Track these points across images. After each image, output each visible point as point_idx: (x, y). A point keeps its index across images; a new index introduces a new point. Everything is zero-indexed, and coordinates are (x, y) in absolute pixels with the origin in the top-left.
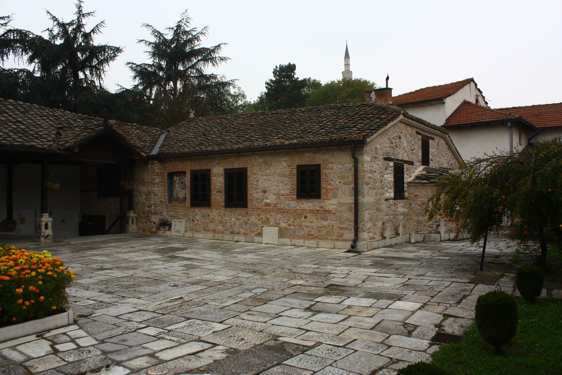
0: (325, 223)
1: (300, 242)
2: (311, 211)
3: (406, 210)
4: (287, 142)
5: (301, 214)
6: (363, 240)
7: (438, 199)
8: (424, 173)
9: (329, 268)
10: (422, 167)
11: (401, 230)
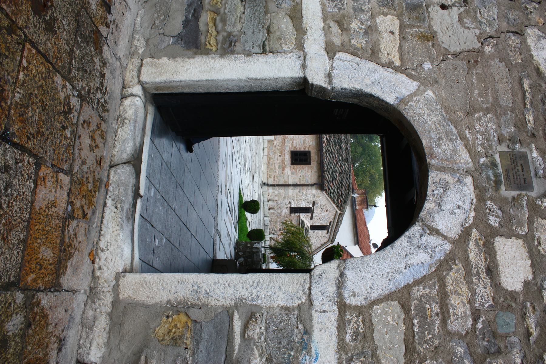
0: (277, 167)
1: (266, 153)
2: (284, 160)
3: (283, 215)
4: (324, 145)
5: (282, 154)
6: (268, 189)
7: (292, 227)
8: (306, 226)
9: (257, 173)
10: (309, 226)
11: (272, 211)
